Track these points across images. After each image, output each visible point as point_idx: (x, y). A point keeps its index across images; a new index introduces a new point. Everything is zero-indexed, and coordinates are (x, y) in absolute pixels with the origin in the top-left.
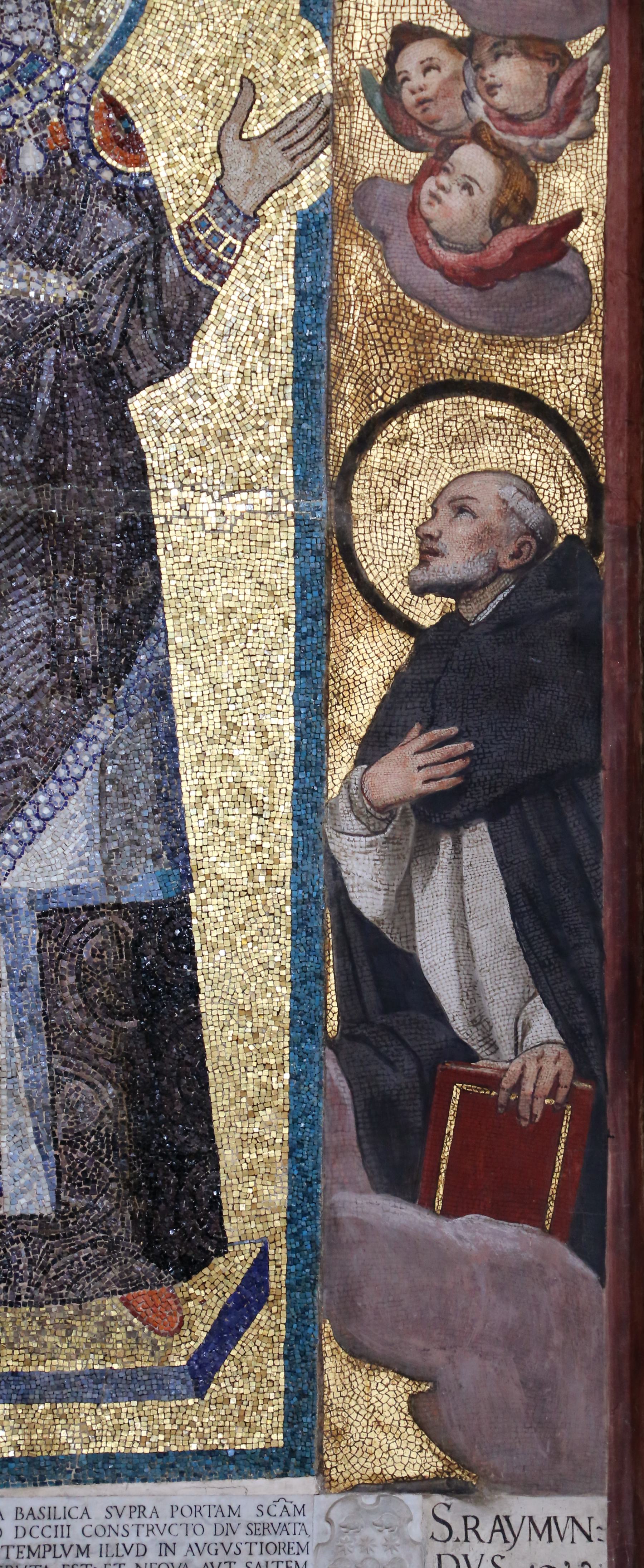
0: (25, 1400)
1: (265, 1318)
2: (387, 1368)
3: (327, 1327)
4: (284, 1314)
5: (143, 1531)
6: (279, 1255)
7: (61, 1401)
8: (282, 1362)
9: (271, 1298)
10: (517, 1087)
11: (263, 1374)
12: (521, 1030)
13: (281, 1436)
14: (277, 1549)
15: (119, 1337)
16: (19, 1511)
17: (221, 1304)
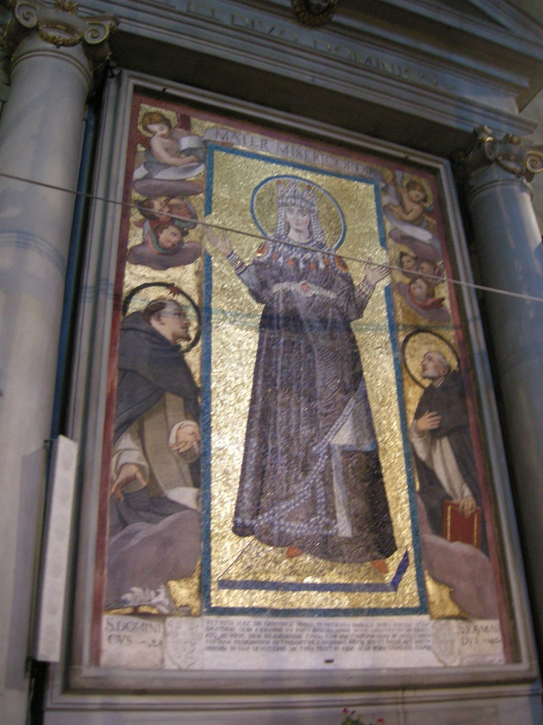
10: (463, 507)
12: (462, 493)
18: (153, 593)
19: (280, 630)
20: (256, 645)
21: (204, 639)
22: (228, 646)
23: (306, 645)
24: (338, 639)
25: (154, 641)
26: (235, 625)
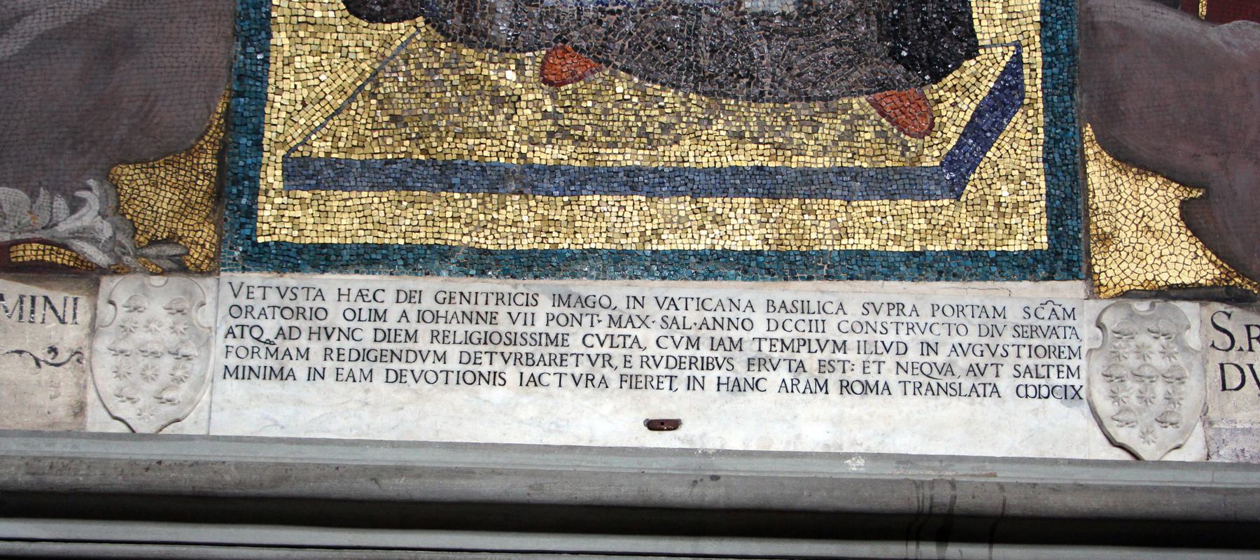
0: (773, 195)
1: (1021, 121)
2: (1155, 173)
3: (1089, 131)
4: (1041, 117)
5: (903, 329)
6: (1034, 57)
7: (810, 197)
8: (1041, 165)
9: (1026, 101)
11: (1023, 176)
13: (1045, 239)
14: (1048, 352)
15: (868, 136)
16: (770, 303)
17: (973, 106)
18: (60, 204)
19: (492, 318)
20: (396, 365)
21: (219, 342)
22: (300, 367)
23: (585, 366)
24: (705, 351)
25: (53, 350)
26: (330, 303)
